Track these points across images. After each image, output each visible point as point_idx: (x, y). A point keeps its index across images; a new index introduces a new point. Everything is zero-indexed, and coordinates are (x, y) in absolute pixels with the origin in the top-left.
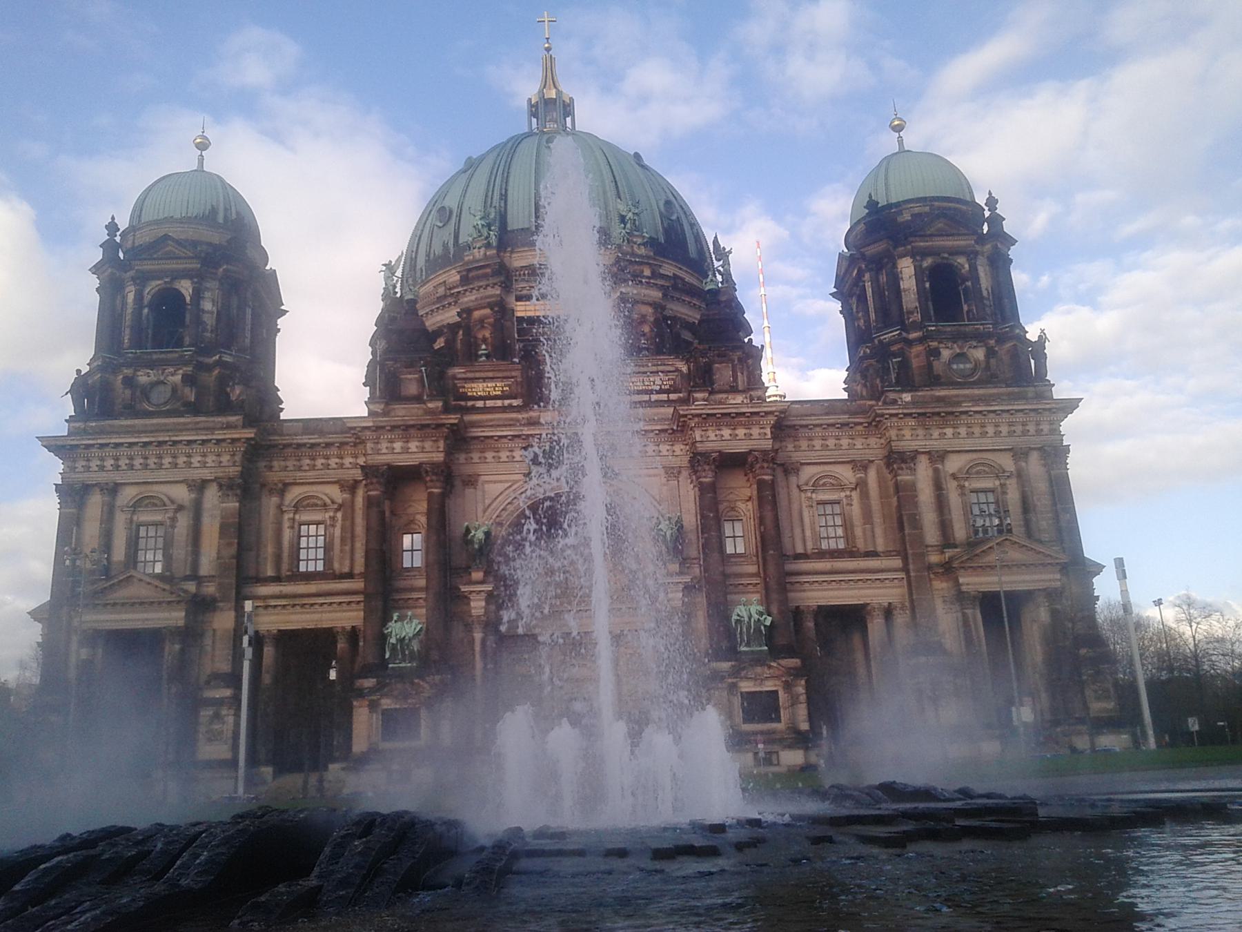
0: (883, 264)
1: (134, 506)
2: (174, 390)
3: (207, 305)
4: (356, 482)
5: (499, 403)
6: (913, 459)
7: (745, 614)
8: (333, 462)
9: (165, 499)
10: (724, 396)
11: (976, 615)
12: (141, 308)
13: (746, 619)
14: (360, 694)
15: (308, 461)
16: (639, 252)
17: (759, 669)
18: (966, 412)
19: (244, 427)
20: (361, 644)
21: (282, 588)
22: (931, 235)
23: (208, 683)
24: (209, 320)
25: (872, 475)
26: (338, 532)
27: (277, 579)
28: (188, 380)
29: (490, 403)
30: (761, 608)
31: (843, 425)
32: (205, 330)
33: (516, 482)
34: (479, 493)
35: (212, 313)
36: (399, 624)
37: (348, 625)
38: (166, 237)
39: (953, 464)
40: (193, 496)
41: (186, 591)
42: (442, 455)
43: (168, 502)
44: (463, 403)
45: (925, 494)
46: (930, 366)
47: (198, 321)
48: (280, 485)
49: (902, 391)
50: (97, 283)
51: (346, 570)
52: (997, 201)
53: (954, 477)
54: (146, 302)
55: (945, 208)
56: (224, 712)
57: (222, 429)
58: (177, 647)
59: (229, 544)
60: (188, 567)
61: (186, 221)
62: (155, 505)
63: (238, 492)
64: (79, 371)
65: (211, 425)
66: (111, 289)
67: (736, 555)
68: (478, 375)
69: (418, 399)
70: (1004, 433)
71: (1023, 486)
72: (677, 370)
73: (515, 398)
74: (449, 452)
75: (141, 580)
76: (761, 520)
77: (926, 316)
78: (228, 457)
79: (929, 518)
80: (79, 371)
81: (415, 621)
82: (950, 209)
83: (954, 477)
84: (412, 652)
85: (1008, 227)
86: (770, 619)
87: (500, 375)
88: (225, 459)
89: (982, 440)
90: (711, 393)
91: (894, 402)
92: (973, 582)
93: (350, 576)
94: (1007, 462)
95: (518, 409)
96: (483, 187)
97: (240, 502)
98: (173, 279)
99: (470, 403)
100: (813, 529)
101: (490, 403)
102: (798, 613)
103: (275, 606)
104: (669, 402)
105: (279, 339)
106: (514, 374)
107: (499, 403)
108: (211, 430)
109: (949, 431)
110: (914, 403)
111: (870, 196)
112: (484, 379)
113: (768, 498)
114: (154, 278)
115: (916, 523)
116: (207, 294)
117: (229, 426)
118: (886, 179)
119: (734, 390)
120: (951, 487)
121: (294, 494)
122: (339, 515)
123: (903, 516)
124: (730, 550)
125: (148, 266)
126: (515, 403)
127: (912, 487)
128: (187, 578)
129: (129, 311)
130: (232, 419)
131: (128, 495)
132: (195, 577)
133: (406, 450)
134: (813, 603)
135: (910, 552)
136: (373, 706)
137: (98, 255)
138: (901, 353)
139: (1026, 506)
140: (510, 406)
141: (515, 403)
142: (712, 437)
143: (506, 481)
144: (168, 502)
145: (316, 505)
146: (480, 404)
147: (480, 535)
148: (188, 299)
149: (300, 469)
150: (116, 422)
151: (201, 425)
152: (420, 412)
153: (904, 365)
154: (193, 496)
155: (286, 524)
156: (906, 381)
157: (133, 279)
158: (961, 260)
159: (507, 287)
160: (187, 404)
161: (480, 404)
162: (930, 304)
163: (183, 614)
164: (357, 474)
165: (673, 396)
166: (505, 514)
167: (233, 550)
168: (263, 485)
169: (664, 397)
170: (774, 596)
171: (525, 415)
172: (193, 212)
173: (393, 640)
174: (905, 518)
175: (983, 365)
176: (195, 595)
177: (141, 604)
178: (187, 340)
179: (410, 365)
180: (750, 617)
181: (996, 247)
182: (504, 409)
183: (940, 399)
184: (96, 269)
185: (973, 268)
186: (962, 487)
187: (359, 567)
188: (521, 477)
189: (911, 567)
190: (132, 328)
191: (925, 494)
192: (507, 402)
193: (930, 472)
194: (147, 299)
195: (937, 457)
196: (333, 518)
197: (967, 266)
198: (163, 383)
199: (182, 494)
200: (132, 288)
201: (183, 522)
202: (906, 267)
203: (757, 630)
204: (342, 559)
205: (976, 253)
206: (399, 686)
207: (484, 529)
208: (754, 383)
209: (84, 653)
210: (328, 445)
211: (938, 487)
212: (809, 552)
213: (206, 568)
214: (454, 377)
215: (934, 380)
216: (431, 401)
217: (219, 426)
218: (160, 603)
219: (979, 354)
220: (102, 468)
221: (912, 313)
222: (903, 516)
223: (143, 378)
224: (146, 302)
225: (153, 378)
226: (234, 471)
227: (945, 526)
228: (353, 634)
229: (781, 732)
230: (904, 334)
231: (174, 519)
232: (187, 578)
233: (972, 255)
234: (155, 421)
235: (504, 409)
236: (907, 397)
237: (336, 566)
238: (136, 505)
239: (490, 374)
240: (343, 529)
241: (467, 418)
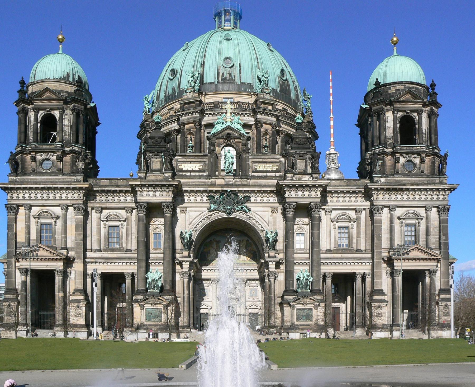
0: (380, 115)
1: (38, 215)
2: (53, 163)
3: (66, 122)
4: (133, 209)
5: (197, 174)
6: (382, 209)
7: (302, 276)
8: (122, 199)
9: (52, 213)
10: (301, 176)
11: (399, 279)
12: (37, 123)
13: (302, 278)
14: (136, 301)
15: (111, 198)
16: (267, 97)
17: (305, 300)
18: (407, 189)
19: (84, 181)
20: (136, 280)
21: (102, 254)
22: (403, 102)
23: (74, 293)
24: (67, 129)
25: (364, 216)
26: (125, 230)
27: (100, 250)
28: (60, 159)
29: (193, 174)
30: (309, 274)
31: (354, 192)
32: (66, 135)
33: (205, 211)
34: (187, 216)
35: (68, 126)
36: (152, 274)
37: (130, 272)
38: (47, 90)
39: (399, 212)
40: (64, 212)
41: (63, 254)
42: (171, 198)
43: (53, 215)
44: (181, 173)
45: (385, 226)
46: (395, 166)
47: (63, 130)
48: (100, 209)
49: (381, 177)
50: (16, 109)
51: (129, 248)
52: (435, 85)
54: (39, 120)
55: (410, 88)
56: (80, 305)
57: (74, 182)
58: (61, 278)
59: (80, 235)
60: (63, 244)
61: (55, 80)
62: (47, 215)
63: (83, 211)
64: (11, 153)
65: (70, 180)
66: (24, 113)
67: (300, 249)
68: (188, 160)
69: (160, 171)
70: (423, 199)
71: (428, 224)
72: (280, 162)
73: (205, 172)
74: (174, 198)
75: (44, 249)
76: (312, 235)
77: (396, 141)
78: (77, 195)
79: (385, 236)
80: (11, 153)
81: (159, 273)
82: (413, 88)
83: (399, 218)
84: (158, 285)
85: (439, 99)
86: (312, 278)
87: (196, 160)
88: (76, 196)
89: (413, 202)
90: (294, 174)
91: (377, 182)
93: (130, 251)
94: (422, 212)
95: (206, 178)
96: (192, 62)
97: (84, 216)
98: (52, 109)
99: (184, 174)
100: (335, 239)
101: (193, 174)
102: (325, 276)
103: (100, 262)
104: (275, 176)
105: (97, 137)
106: (204, 160)
107: (197, 174)
108: (70, 182)
109: (399, 197)
110: (385, 183)
111: (377, 79)
112: (191, 162)
113: (315, 224)
114: (42, 110)
115: (380, 239)
116: (66, 117)
117: (78, 181)
118: (386, 68)
119: (305, 173)
120: (396, 222)
121: (105, 212)
122: (125, 223)
123: (374, 236)
124: (297, 246)
125: (40, 103)
126: (205, 174)
128: (62, 248)
129: (32, 124)
130: (79, 177)
131: (35, 211)
132: (66, 248)
133: (155, 196)
134: (332, 272)
135: (375, 251)
136: (142, 307)
137: (16, 97)
138: (383, 159)
139: (427, 232)
140: (202, 176)
141: (205, 174)
142: (293, 195)
143: (200, 211)
144: (53, 215)
145: (115, 218)
146: (188, 174)
147: (187, 236)
148: (58, 120)
149: (108, 201)
150: (29, 177)
151: (64, 180)
152: (161, 178)
153: (383, 164)
154: (64, 212)
155: (103, 226)
156: (383, 174)
157: (33, 109)
158: (415, 114)
159: (202, 113)
160: (59, 170)
161: (188, 174)
162: (398, 135)
163: (62, 264)
164: (134, 205)
165: (277, 174)
166: (198, 227)
167: (81, 237)
168: (93, 209)
169: (273, 174)
170: (315, 269)
171: (209, 180)
172: (58, 76)
173: (150, 280)
174: (375, 236)
175: (418, 166)
176: (67, 256)
177: (45, 259)
178: (58, 139)
179: (156, 155)
180: (304, 277)
181: (432, 109)
182: (200, 177)
183: (398, 182)
184: (18, 103)
185: (420, 118)
186: (401, 223)
187: (134, 246)
188: (206, 209)
189: (375, 257)
190: (34, 133)
191: (385, 226)
192: (201, 174)
193: (389, 215)
194: (40, 118)
195: (391, 209)
196: (122, 224)
197: (417, 117)
198: (48, 159)
199: (58, 211)
200: (33, 113)
201: (59, 223)
202: (389, 116)
203: (306, 283)
204: (127, 244)
205: (422, 111)
206: (153, 299)
207: (189, 233)
208: (315, 169)
209: (23, 278)
210: (121, 191)
211: (391, 222)
212: (332, 249)
213: (70, 244)
214: (177, 161)
215: (395, 172)
216: (166, 173)
217: (73, 180)
218: (53, 259)
219: (417, 161)
220: (24, 198)
221: (390, 139)
222: (374, 236)
223: (39, 157)
224: (39, 120)
225: (44, 157)
226: (81, 201)
227: (391, 240)
228: (133, 276)
229: (312, 325)
230: (386, 150)
231: (55, 222)
232: (62, 248)
233: (419, 112)
234: (45, 177)
235: (200, 177)
236: (383, 180)
237: (124, 246)
238: (39, 216)
239: (193, 160)
240: (127, 229)
241: (182, 181)
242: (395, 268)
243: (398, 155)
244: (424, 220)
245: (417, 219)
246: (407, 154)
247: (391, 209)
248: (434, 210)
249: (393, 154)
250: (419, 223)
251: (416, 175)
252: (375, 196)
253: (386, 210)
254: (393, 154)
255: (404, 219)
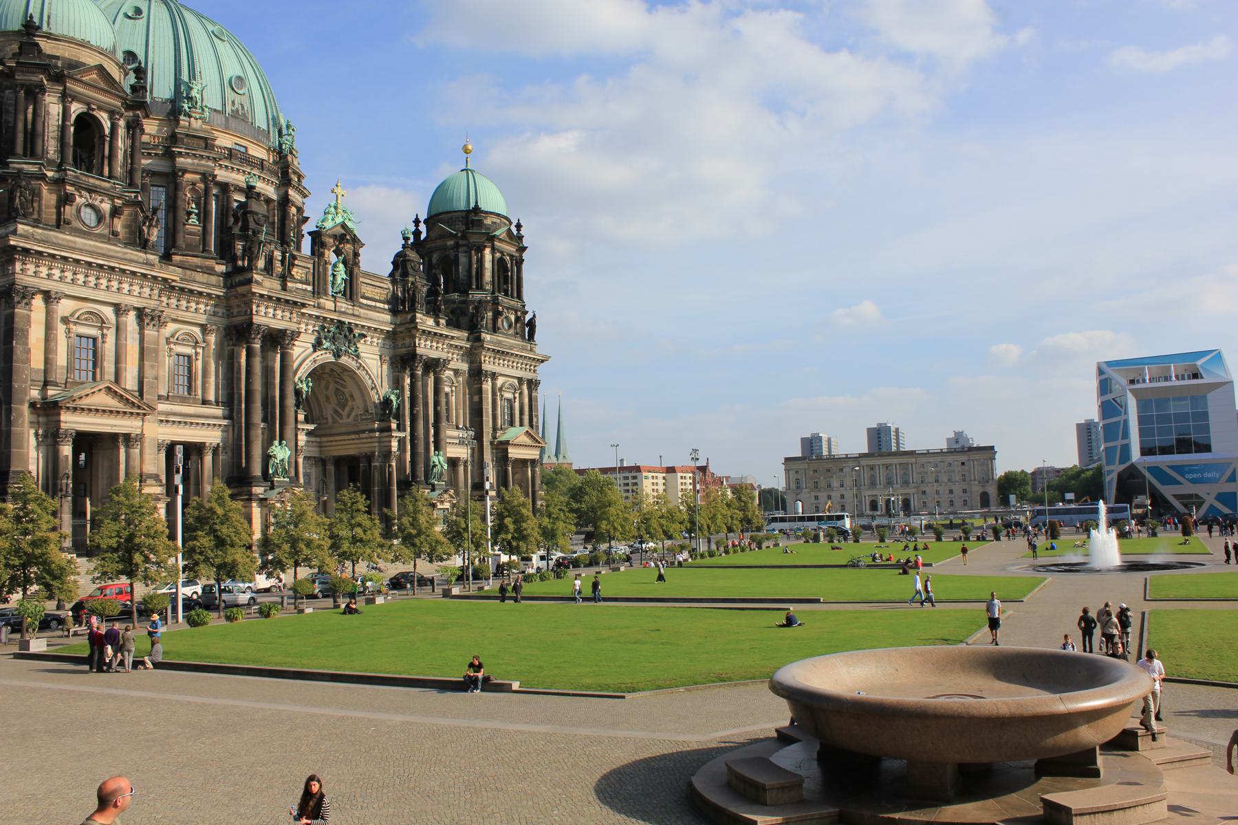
11: (67, 450)
39: (65, 307)
53: (65, 320)
83: (65, 320)
92: (71, 421)
127: (28, 320)
211: (49, 327)
242: (63, 426)
243: (70, 189)
244: (113, 330)
245: (101, 328)
246: (90, 191)
247: (47, 296)
248: (132, 314)
249: (59, 183)
250: (103, 336)
251: (99, 237)
252: (18, 266)
253: (38, 302)
254: (59, 183)
255: (75, 323)
